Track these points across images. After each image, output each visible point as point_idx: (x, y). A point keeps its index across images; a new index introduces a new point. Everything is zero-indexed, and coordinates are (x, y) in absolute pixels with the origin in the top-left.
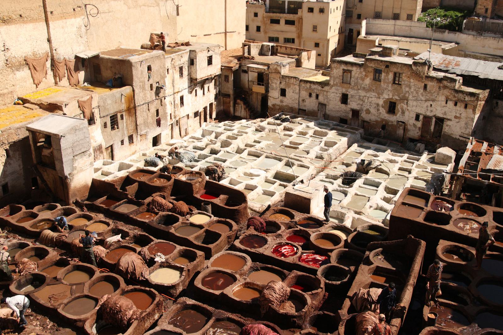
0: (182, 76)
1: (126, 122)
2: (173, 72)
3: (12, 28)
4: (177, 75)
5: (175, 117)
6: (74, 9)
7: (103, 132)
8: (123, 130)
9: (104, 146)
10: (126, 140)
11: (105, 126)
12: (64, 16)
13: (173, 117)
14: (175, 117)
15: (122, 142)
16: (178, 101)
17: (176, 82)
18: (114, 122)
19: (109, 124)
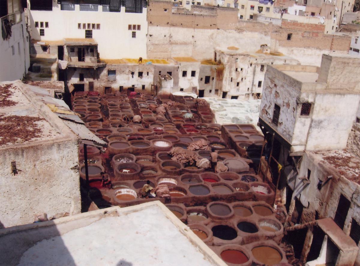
0: (263, 70)
1: (216, 83)
2: (255, 67)
3: (176, 29)
4: (258, 69)
5: (252, 91)
6: (211, 26)
7: (199, 82)
8: (212, 86)
9: (198, 89)
10: (213, 91)
11: (201, 79)
12: (204, 27)
13: (250, 89)
14: (252, 91)
15: (210, 91)
16: (257, 84)
17: (256, 72)
18: (207, 80)
19: (204, 80)
